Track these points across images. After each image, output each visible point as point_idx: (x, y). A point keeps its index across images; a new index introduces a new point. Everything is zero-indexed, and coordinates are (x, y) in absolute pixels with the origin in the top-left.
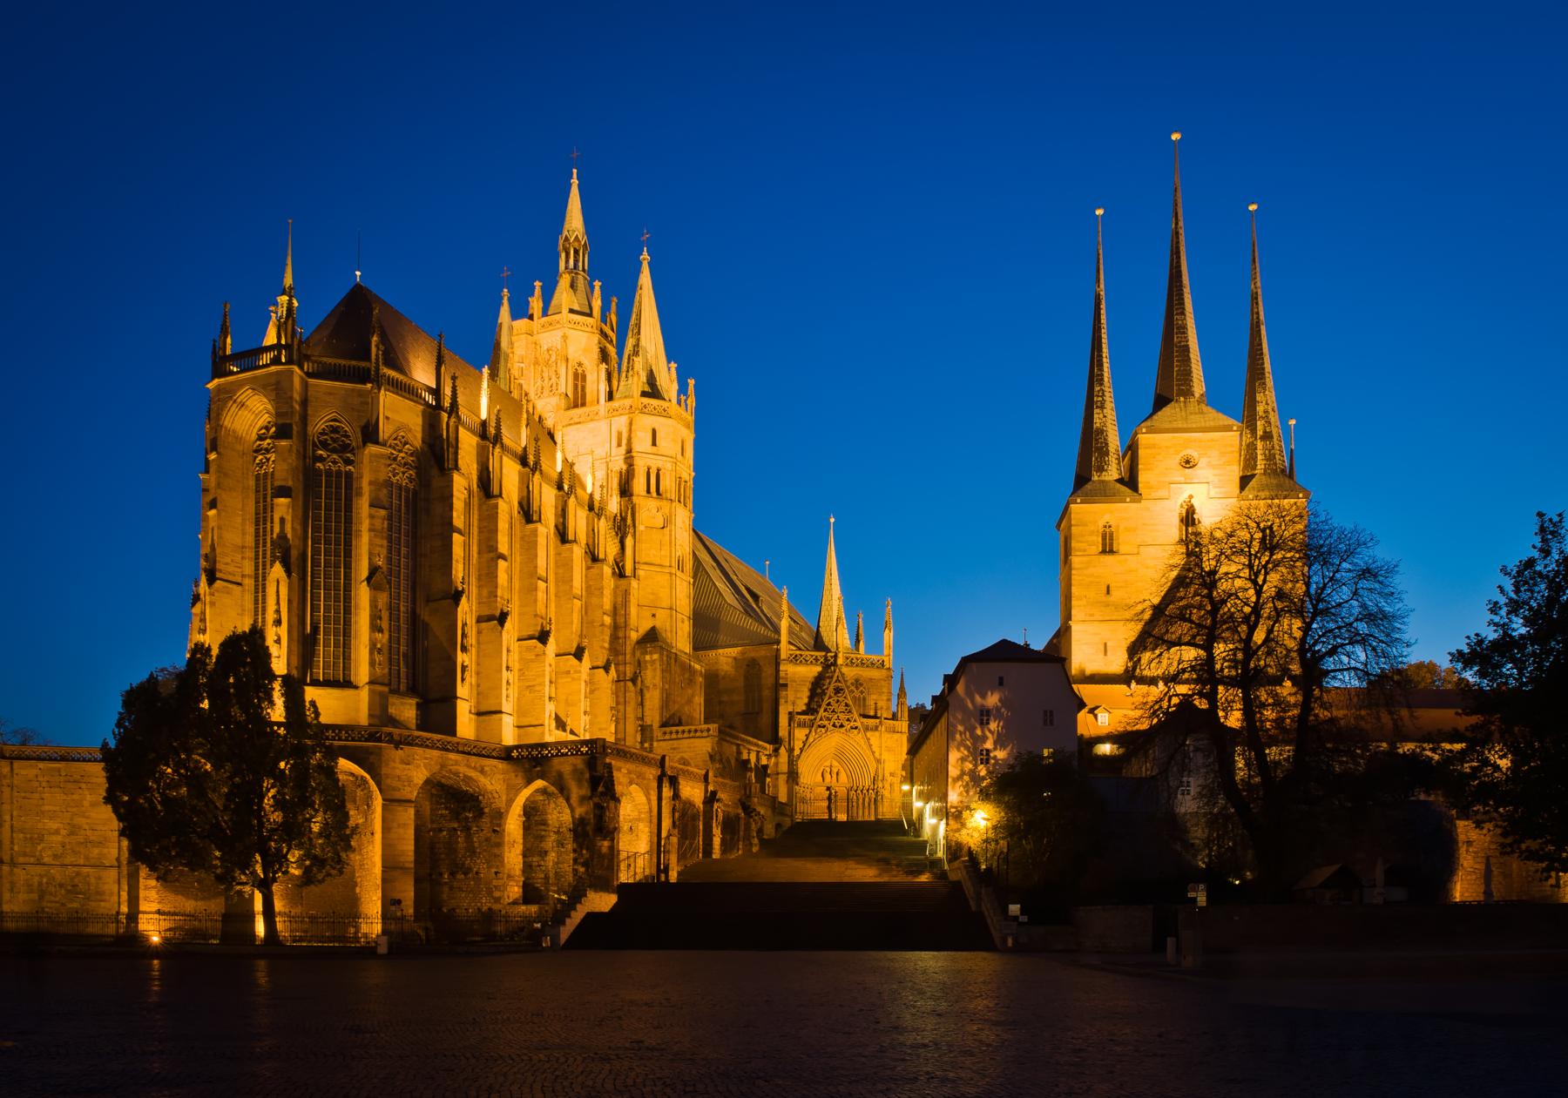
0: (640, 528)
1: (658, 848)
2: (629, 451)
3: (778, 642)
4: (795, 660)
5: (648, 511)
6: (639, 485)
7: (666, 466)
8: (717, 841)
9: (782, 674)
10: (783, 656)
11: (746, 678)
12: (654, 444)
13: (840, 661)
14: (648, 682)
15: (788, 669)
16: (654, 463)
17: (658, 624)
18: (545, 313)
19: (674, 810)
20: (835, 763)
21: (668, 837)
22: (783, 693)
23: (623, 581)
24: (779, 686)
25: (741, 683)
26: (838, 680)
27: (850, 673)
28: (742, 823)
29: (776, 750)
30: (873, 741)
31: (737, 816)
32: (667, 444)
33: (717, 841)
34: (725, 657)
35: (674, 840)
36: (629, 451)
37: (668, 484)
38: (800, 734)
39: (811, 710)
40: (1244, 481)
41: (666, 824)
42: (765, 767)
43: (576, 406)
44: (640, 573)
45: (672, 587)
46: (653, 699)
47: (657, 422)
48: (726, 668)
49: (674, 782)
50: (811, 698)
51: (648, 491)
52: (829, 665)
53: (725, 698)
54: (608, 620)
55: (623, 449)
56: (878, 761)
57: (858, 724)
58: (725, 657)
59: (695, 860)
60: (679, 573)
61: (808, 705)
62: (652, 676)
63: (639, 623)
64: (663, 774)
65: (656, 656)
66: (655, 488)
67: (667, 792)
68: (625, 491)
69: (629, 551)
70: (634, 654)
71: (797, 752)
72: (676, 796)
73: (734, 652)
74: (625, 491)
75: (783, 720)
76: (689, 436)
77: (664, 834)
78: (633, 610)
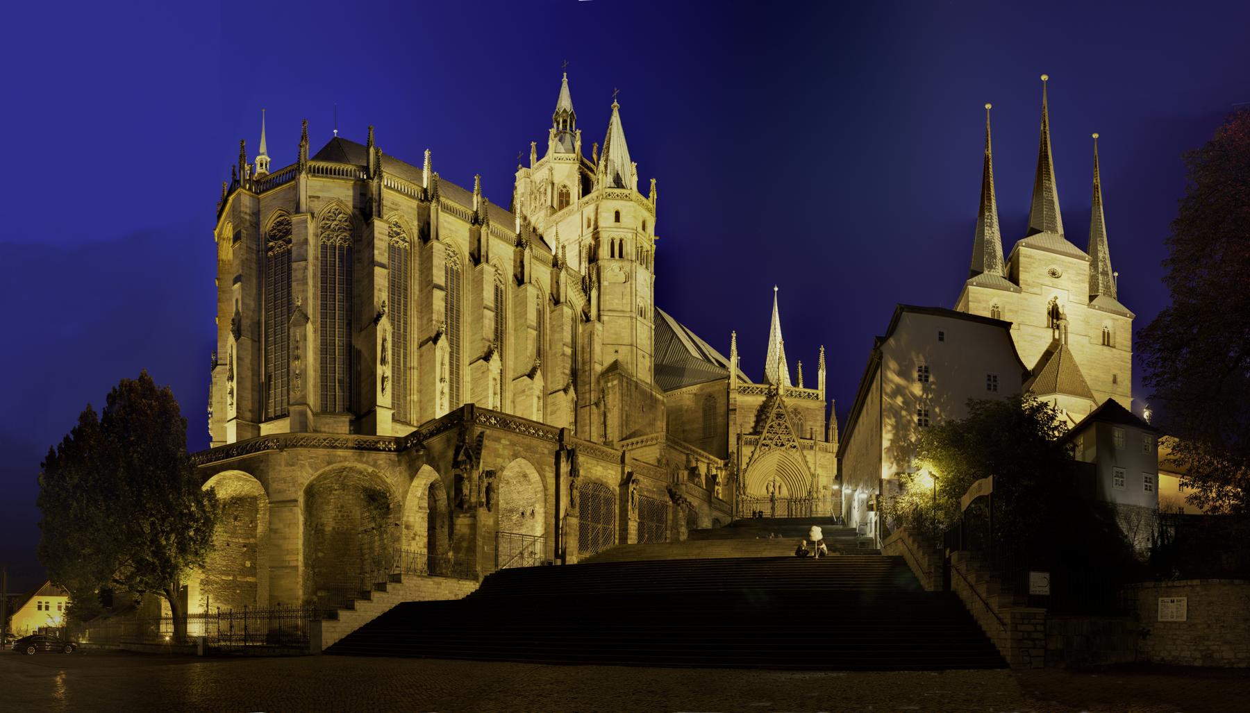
0: (605, 283)
1: (556, 530)
2: (596, 228)
4: (743, 391)
5: (612, 270)
6: (604, 252)
7: (628, 237)
8: (633, 526)
9: (731, 401)
10: (732, 386)
11: (704, 410)
13: (781, 392)
14: (610, 406)
15: (738, 399)
16: (617, 235)
17: (620, 357)
19: (571, 487)
21: (565, 518)
22: (732, 417)
23: (589, 325)
24: (730, 410)
25: (700, 414)
26: (779, 407)
27: (790, 402)
28: (670, 511)
31: (664, 506)
33: (633, 526)
34: (687, 395)
35: (574, 521)
36: (596, 228)
37: (629, 249)
38: (747, 451)
39: (756, 432)
41: (564, 502)
42: (715, 477)
43: (561, 207)
44: (605, 318)
45: (633, 328)
46: (614, 420)
48: (688, 403)
49: (571, 455)
50: (757, 422)
51: (613, 256)
52: (771, 395)
53: (687, 427)
54: (568, 351)
55: (591, 229)
58: (687, 395)
59: (609, 546)
60: (639, 318)
61: (755, 428)
62: (613, 400)
63: (602, 358)
64: (562, 448)
65: (615, 382)
66: (618, 251)
67: (565, 468)
68: (593, 258)
70: (598, 382)
71: (744, 466)
72: (574, 472)
73: (694, 389)
74: (593, 258)
75: (732, 440)
77: (562, 515)
78: (597, 348)
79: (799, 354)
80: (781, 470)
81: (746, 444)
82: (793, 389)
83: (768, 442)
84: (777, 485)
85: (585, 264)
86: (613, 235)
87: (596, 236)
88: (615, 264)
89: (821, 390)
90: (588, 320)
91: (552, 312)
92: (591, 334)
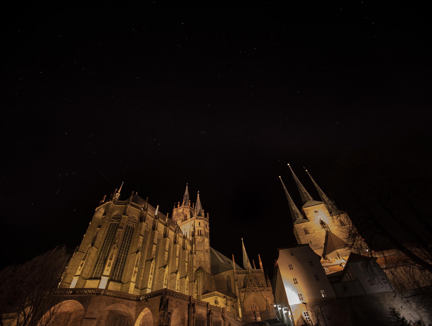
2: (194, 227)
3: (233, 269)
4: (238, 273)
5: (199, 239)
6: (196, 234)
9: (235, 277)
10: (235, 272)
12: (200, 225)
13: (250, 272)
18: (180, 206)
20: (254, 303)
29: (236, 301)
30: (263, 294)
32: (202, 225)
36: (194, 227)
37: (202, 232)
39: (244, 287)
40: (330, 213)
44: (197, 253)
47: (200, 221)
50: (244, 283)
56: (266, 301)
57: (258, 289)
68: (193, 235)
69: (194, 248)
74: (193, 235)
75: (237, 291)
76: (208, 224)
78: (195, 263)
79: (252, 258)
80: (255, 300)
81: (242, 292)
82: (253, 270)
83: (248, 290)
84: (255, 306)
85: (191, 237)
86: (199, 229)
87: (194, 229)
88: (199, 237)
89: (262, 269)
90: (192, 254)
91: (182, 252)
92: (193, 258)
